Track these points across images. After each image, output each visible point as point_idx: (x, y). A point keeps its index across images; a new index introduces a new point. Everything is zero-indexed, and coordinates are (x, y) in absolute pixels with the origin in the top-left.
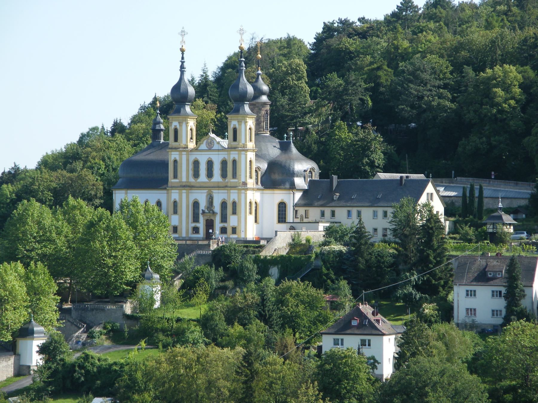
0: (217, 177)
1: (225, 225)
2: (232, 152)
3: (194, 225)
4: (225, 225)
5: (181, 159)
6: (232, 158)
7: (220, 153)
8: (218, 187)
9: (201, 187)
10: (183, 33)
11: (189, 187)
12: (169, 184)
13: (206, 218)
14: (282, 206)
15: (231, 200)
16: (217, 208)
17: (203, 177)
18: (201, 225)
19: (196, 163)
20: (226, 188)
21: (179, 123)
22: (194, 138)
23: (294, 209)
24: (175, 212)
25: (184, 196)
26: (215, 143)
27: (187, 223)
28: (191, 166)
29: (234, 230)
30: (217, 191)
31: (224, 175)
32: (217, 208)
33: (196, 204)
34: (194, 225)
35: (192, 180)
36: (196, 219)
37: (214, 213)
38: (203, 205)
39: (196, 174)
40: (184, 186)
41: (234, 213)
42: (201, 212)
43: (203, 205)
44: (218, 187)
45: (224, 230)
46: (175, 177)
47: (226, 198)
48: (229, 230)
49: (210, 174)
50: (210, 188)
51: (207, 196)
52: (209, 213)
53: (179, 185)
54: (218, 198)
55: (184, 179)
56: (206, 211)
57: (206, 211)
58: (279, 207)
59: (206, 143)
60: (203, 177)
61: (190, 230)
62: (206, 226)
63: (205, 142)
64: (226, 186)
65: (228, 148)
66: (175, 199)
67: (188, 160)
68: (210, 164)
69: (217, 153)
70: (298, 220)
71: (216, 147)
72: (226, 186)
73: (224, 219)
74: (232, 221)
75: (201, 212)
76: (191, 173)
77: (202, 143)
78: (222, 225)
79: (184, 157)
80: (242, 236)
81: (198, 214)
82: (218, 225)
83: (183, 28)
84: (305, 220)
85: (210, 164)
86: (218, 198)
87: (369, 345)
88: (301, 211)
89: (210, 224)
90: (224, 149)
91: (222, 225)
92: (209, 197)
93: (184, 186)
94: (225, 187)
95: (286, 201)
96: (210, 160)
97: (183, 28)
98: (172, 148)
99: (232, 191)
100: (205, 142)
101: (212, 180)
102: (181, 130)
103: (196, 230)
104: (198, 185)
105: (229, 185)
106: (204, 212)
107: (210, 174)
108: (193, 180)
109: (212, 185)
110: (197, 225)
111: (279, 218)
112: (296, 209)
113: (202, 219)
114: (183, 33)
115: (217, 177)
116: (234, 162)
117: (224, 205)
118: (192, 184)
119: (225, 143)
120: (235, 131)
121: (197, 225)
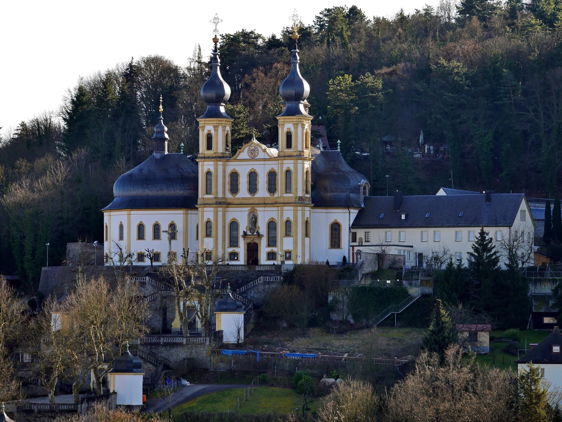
0: (262, 191)
1: (275, 249)
2: (285, 161)
3: (231, 250)
5: (216, 170)
6: (285, 168)
7: (266, 162)
9: (241, 204)
11: (223, 203)
12: (199, 201)
13: (248, 241)
14: (335, 228)
18: (242, 250)
20: (276, 205)
22: (230, 145)
24: (208, 235)
27: (224, 248)
28: (228, 180)
30: (262, 209)
31: (272, 188)
33: (234, 225)
34: (231, 250)
35: (229, 195)
36: (234, 242)
37: (259, 236)
38: (243, 226)
39: (234, 189)
40: (220, 203)
42: (241, 233)
43: (243, 226)
44: (264, 204)
45: (271, 256)
46: (208, 191)
47: (276, 218)
49: (253, 188)
50: (253, 205)
51: (249, 214)
53: (214, 201)
54: (264, 216)
55: (220, 195)
56: (249, 233)
57: (249, 233)
61: (227, 256)
62: (248, 250)
63: (246, 149)
65: (279, 156)
67: (224, 171)
68: (253, 176)
69: (262, 162)
71: (261, 155)
72: (276, 203)
74: (287, 244)
75: (241, 233)
76: (228, 187)
77: (243, 152)
78: (269, 249)
79: (220, 168)
80: (299, 262)
82: (264, 250)
83: (216, 14)
84: (364, 244)
85: (253, 176)
86: (264, 216)
88: (361, 233)
89: (253, 250)
90: (274, 159)
91: (269, 249)
92: (251, 215)
93: (220, 203)
94: (275, 204)
95: (339, 221)
96: (253, 171)
97: (216, 14)
98: (204, 158)
101: (256, 196)
102: (217, 135)
103: (234, 256)
105: (281, 200)
106: (245, 234)
107: (253, 188)
110: (236, 250)
115: (262, 191)
117: (272, 225)
118: (229, 201)
119: (274, 152)
120: (289, 136)
121: (236, 250)
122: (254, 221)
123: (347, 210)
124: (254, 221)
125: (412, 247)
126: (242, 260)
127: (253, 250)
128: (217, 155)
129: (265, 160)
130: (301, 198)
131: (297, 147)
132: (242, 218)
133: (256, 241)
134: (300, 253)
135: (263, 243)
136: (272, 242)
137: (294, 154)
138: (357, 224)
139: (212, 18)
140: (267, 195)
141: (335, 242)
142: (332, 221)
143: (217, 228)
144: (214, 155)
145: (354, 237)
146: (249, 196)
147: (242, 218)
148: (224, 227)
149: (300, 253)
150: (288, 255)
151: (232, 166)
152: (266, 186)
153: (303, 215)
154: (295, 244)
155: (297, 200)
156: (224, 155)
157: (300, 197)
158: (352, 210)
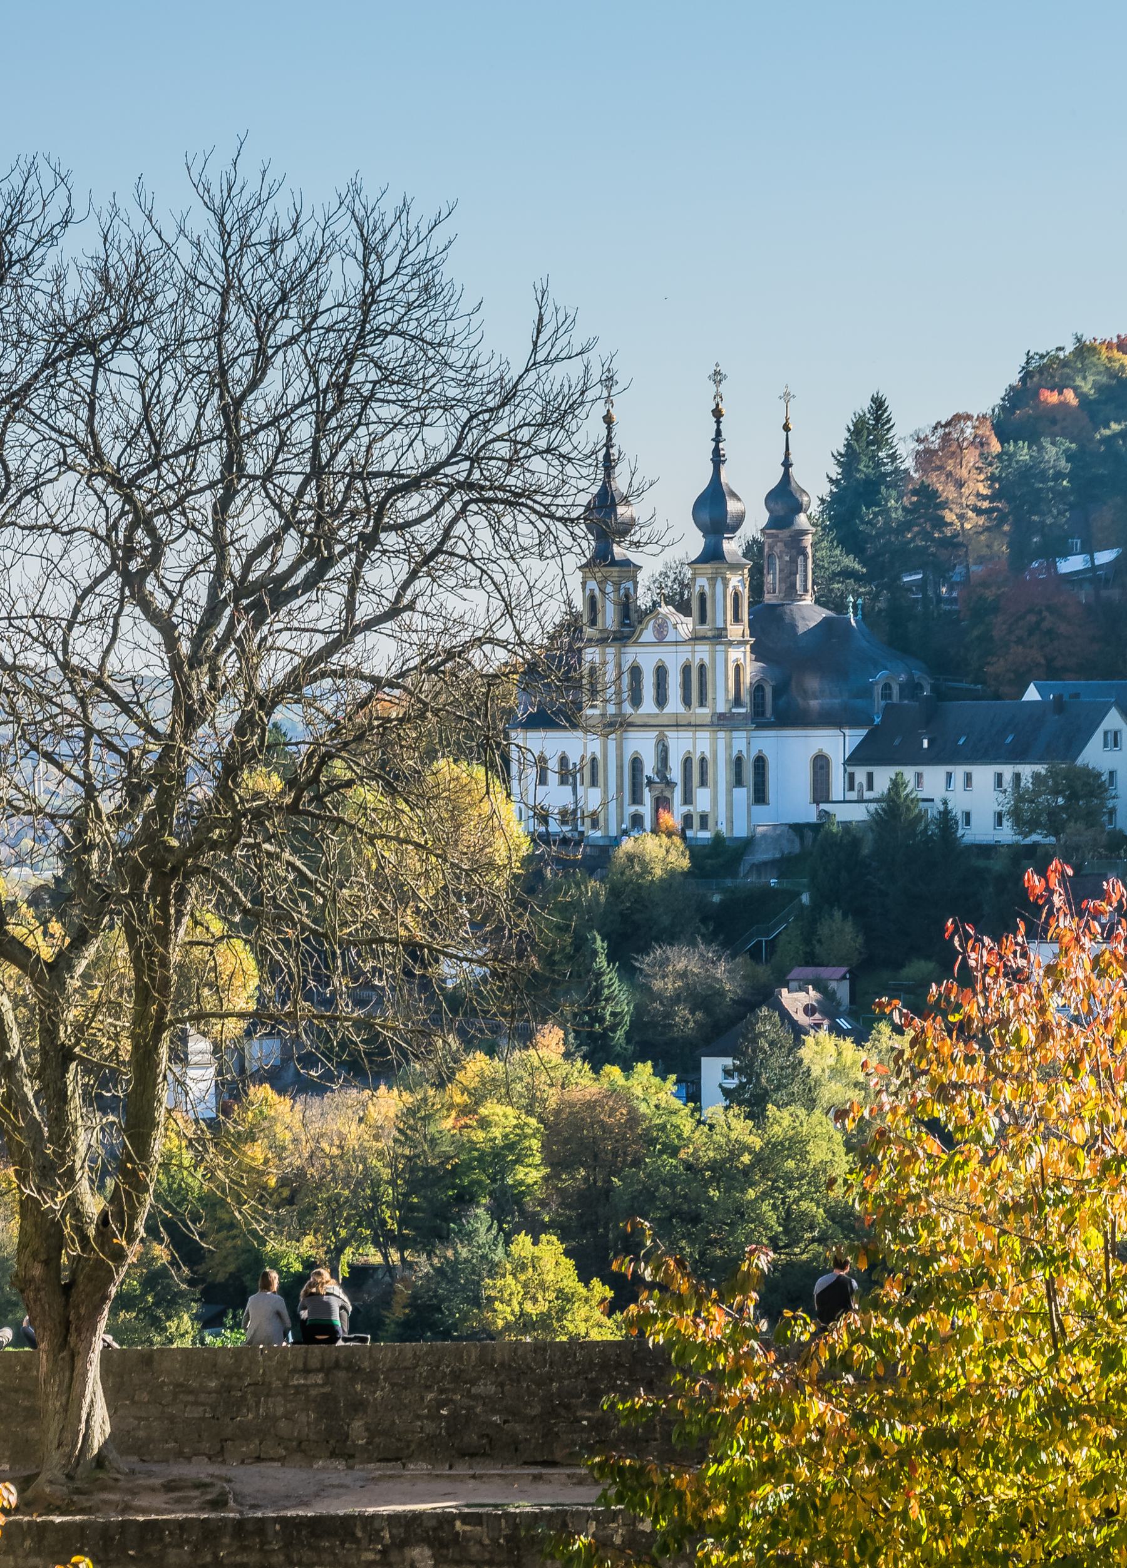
0: (675, 704)
3: (633, 809)
4: (691, 808)
7: (680, 648)
14: (821, 764)
15: (698, 755)
16: (676, 773)
17: (648, 706)
19: (636, 672)
24: (594, 783)
25: (612, 745)
26: (670, 627)
27: (621, 806)
29: (704, 818)
31: (687, 701)
32: (676, 773)
33: (637, 764)
34: (633, 809)
35: (628, 709)
36: (637, 799)
37: (670, 784)
38: (649, 769)
39: (636, 701)
41: (703, 783)
44: (677, 725)
48: (696, 822)
49: (661, 699)
60: (648, 706)
67: (619, 665)
68: (661, 672)
69: (673, 648)
70: (853, 795)
73: (688, 799)
74: (703, 799)
78: (685, 809)
85: (661, 672)
95: (826, 751)
104: (638, 721)
107: (661, 699)
112: (850, 769)
113: (647, 796)
115: (675, 704)
130: (721, 716)
133: (667, 794)
134: (722, 818)
138: (855, 759)
140: (681, 709)
142: (814, 752)
146: (656, 711)
148: (620, 768)
150: (704, 818)
153: (729, 746)
157: (721, 714)
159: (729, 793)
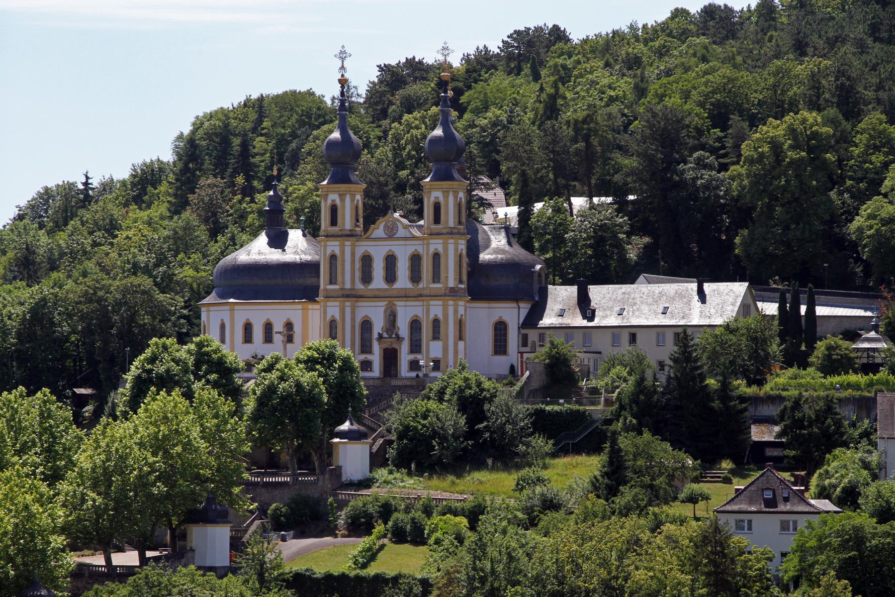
0: (403, 281)
3: (363, 357)
5: (343, 252)
6: (432, 250)
7: (408, 242)
8: (405, 295)
9: (376, 296)
10: (343, 55)
13: (385, 346)
14: (500, 329)
16: (403, 329)
17: (378, 281)
18: (376, 358)
19: (367, 260)
21: (340, 195)
22: (361, 220)
23: (519, 332)
28: (358, 265)
30: (403, 303)
31: (415, 277)
32: (403, 329)
33: (366, 325)
35: (359, 286)
36: (366, 348)
37: (399, 339)
38: (378, 326)
39: (367, 278)
40: (348, 296)
42: (375, 335)
43: (378, 326)
46: (332, 281)
47: (420, 315)
49: (390, 276)
51: (385, 311)
52: (390, 337)
53: (340, 293)
54: (405, 313)
55: (348, 286)
56: (385, 335)
57: (385, 335)
58: (496, 329)
59: (385, 227)
60: (378, 281)
62: (384, 358)
63: (382, 226)
64: (421, 296)
66: (436, 315)
67: (353, 254)
68: (391, 261)
69: (403, 242)
71: (401, 233)
72: (421, 296)
73: (416, 347)
74: (435, 349)
75: (375, 335)
76: (358, 274)
77: (378, 228)
78: (412, 357)
79: (348, 250)
81: (371, 341)
82: (405, 357)
83: (343, 47)
85: (391, 261)
86: (405, 313)
87: (750, 528)
89: (390, 357)
91: (412, 357)
92: (388, 312)
94: (419, 296)
95: (505, 318)
97: (343, 47)
99: (432, 303)
100: (382, 226)
101: (395, 286)
102: (344, 207)
104: (370, 294)
106: (380, 336)
107: (390, 276)
108: (362, 287)
109: (395, 293)
110: (369, 357)
111: (495, 346)
112: (523, 331)
113: (376, 348)
114: (343, 55)
115: (403, 281)
116: (436, 256)
117: (415, 326)
120: (437, 207)
121: (369, 357)
122: (392, 319)
123: (515, 305)
124: (392, 319)
125: (600, 353)
126: (377, 371)
127: (390, 357)
128: (345, 233)
129: (406, 239)
131: (447, 221)
132: (377, 314)
133: (395, 346)
135: (405, 347)
136: (416, 347)
137: (444, 231)
139: (337, 52)
140: (409, 285)
141: (500, 347)
142: (495, 319)
143: (344, 329)
144: (340, 233)
145: (524, 341)
146: (386, 287)
147: (377, 314)
148: (353, 327)
149: (451, 362)
151: (363, 248)
152: (407, 273)
153: (456, 312)
154: (445, 349)
155: (447, 292)
156: (354, 233)
158: (522, 305)
159: (456, 345)
